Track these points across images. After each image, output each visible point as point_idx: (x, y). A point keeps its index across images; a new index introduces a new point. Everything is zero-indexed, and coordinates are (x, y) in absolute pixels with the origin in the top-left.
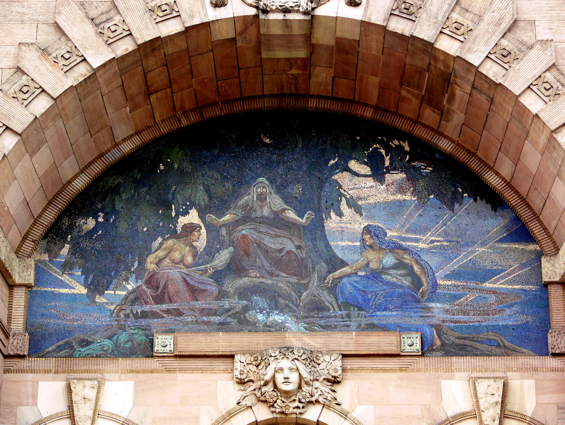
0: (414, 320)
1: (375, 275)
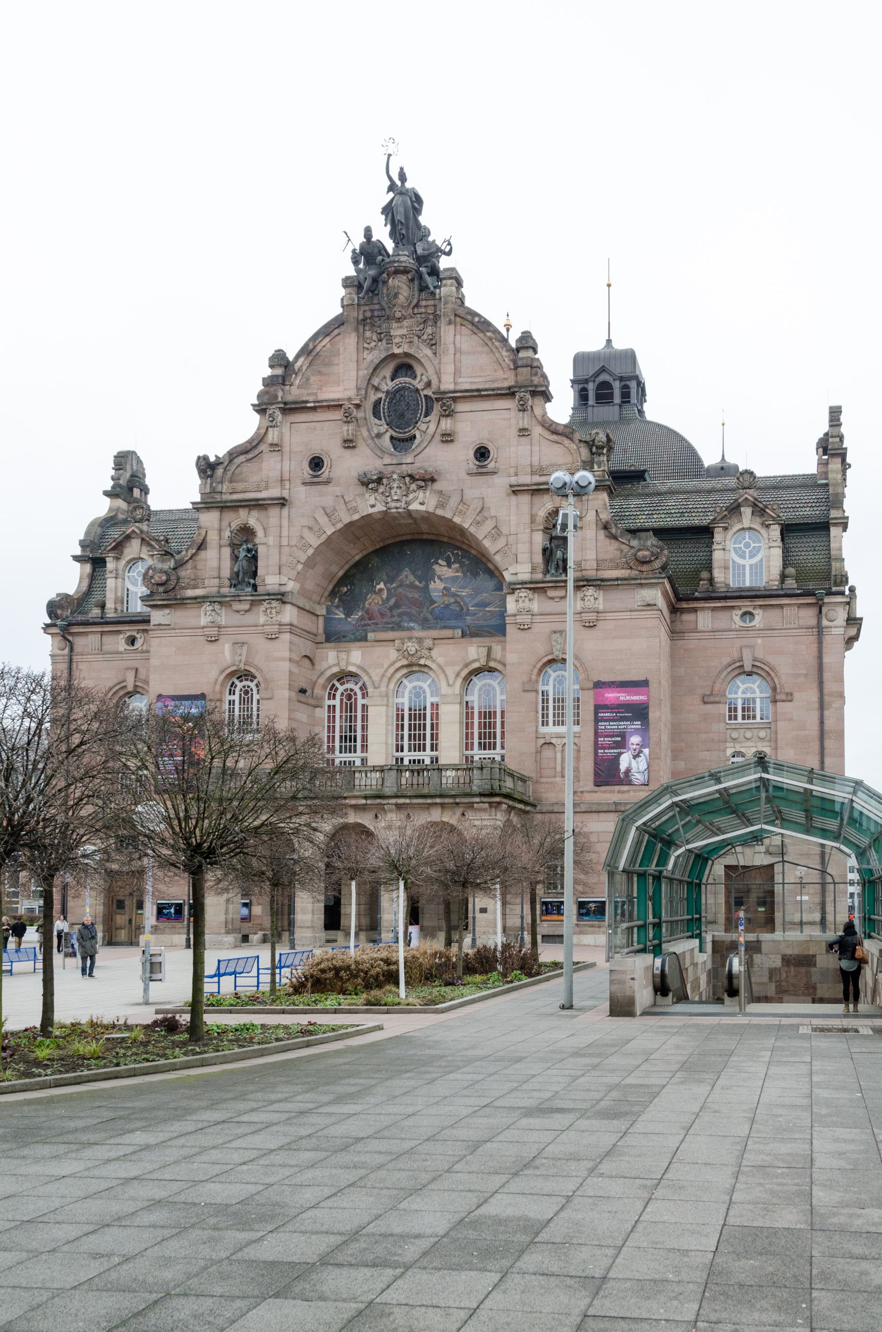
0: (461, 624)
1: (447, 606)
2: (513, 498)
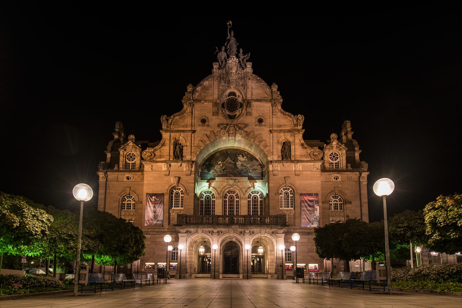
2: (271, 135)
